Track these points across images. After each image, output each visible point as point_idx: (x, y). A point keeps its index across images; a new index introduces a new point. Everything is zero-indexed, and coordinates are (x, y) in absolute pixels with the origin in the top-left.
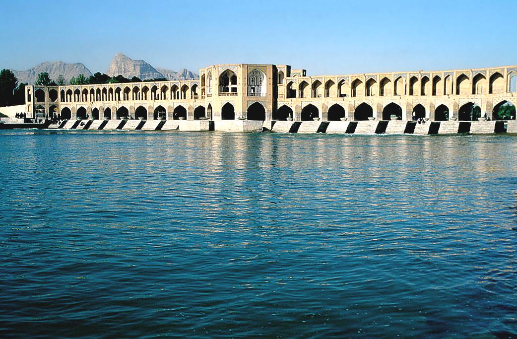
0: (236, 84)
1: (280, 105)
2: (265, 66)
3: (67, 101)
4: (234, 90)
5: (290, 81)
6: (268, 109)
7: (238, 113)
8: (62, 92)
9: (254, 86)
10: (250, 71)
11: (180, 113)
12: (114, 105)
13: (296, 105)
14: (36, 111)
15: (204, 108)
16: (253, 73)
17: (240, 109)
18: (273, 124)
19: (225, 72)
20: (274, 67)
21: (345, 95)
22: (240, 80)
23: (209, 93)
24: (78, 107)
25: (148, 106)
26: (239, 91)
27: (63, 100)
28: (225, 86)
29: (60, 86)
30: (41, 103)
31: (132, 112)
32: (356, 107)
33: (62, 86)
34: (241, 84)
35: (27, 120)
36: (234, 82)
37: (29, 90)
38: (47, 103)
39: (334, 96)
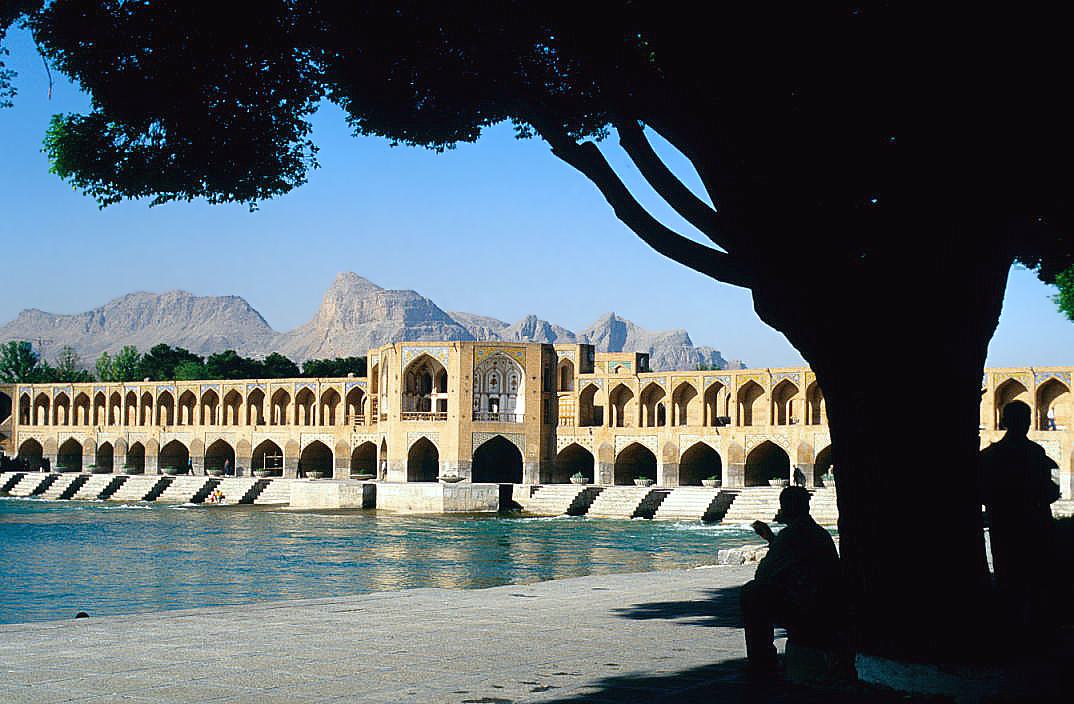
0: (444, 390)
1: (563, 442)
3: (35, 423)
4: (443, 404)
5: (590, 382)
6: (530, 452)
7: (447, 465)
8: (25, 399)
9: (497, 396)
10: (482, 357)
11: (317, 461)
12: (153, 435)
13: (604, 443)
15: (375, 446)
18: (533, 490)
19: (415, 362)
21: (726, 421)
22: (453, 383)
23: (384, 412)
26: (453, 408)
28: (422, 395)
29: (19, 385)
31: (196, 454)
32: (748, 450)
33: (24, 385)
34: (457, 392)
39: (695, 423)
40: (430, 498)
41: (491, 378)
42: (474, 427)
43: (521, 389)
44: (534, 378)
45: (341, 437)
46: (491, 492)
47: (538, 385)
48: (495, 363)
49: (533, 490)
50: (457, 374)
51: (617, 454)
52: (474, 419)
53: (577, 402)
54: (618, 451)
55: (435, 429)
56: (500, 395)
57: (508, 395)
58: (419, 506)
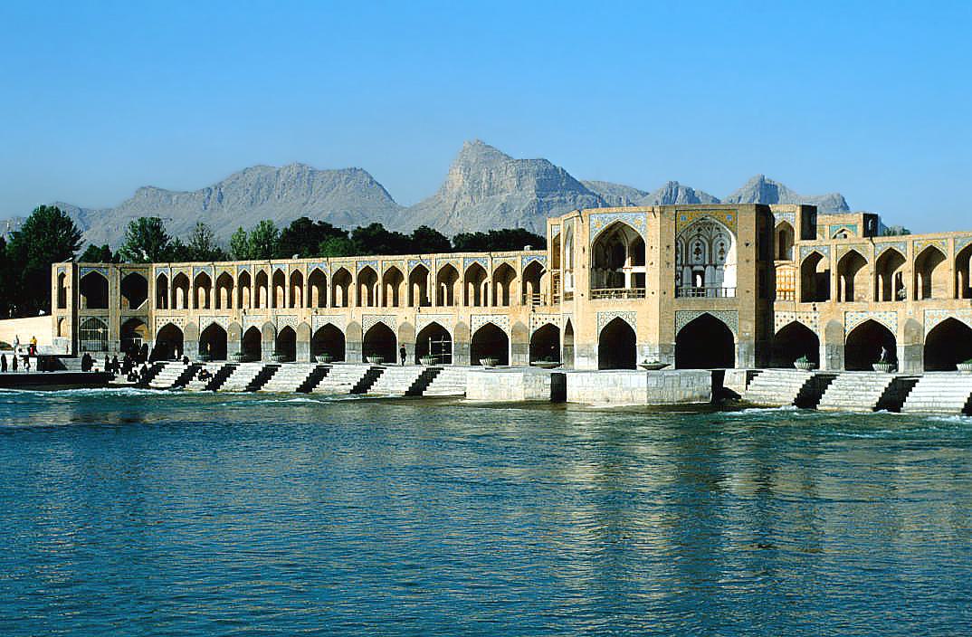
0: (643, 264)
1: (781, 320)
3: (174, 306)
4: (640, 280)
6: (743, 332)
7: (646, 348)
8: (162, 280)
11: (490, 346)
12: (304, 319)
14: (80, 333)
16: (699, 230)
18: (750, 376)
19: (611, 228)
22: (652, 254)
23: (568, 290)
25: (399, 324)
26: (652, 284)
27: (162, 304)
28: (614, 270)
29: (154, 265)
30: (96, 313)
31: (353, 340)
33: (160, 265)
35: (48, 362)
36: (639, 259)
37: (61, 277)
38: (115, 311)
40: (630, 388)
41: (695, 247)
43: (732, 256)
44: (747, 245)
45: (516, 319)
46: (697, 383)
47: (752, 252)
48: (699, 230)
49: (750, 376)
51: (847, 334)
52: (677, 296)
53: (798, 272)
54: (849, 330)
55: (630, 308)
56: (705, 267)
57: (715, 266)
58: (618, 397)
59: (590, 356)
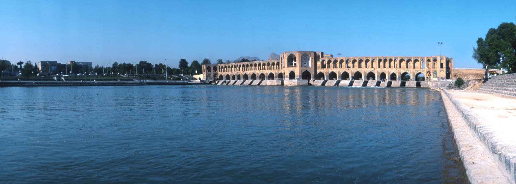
1: (318, 72)
2: (310, 52)
4: (295, 64)
5: (323, 59)
6: (312, 74)
8: (219, 67)
11: (271, 76)
12: (241, 73)
13: (326, 71)
14: (208, 76)
17: (297, 73)
20: (315, 53)
22: (297, 59)
24: (226, 74)
26: (298, 65)
27: (219, 71)
30: (209, 73)
31: (249, 76)
32: (354, 73)
34: (298, 61)
35: (202, 81)
36: (295, 61)
37: (204, 67)
38: (212, 73)
39: (344, 68)
40: (294, 82)
41: (304, 59)
42: (302, 68)
43: (310, 61)
45: (275, 72)
46: (306, 81)
47: (313, 60)
49: (314, 81)
50: (298, 58)
53: (321, 63)
55: (294, 69)
58: (292, 84)
59: (287, 77)
